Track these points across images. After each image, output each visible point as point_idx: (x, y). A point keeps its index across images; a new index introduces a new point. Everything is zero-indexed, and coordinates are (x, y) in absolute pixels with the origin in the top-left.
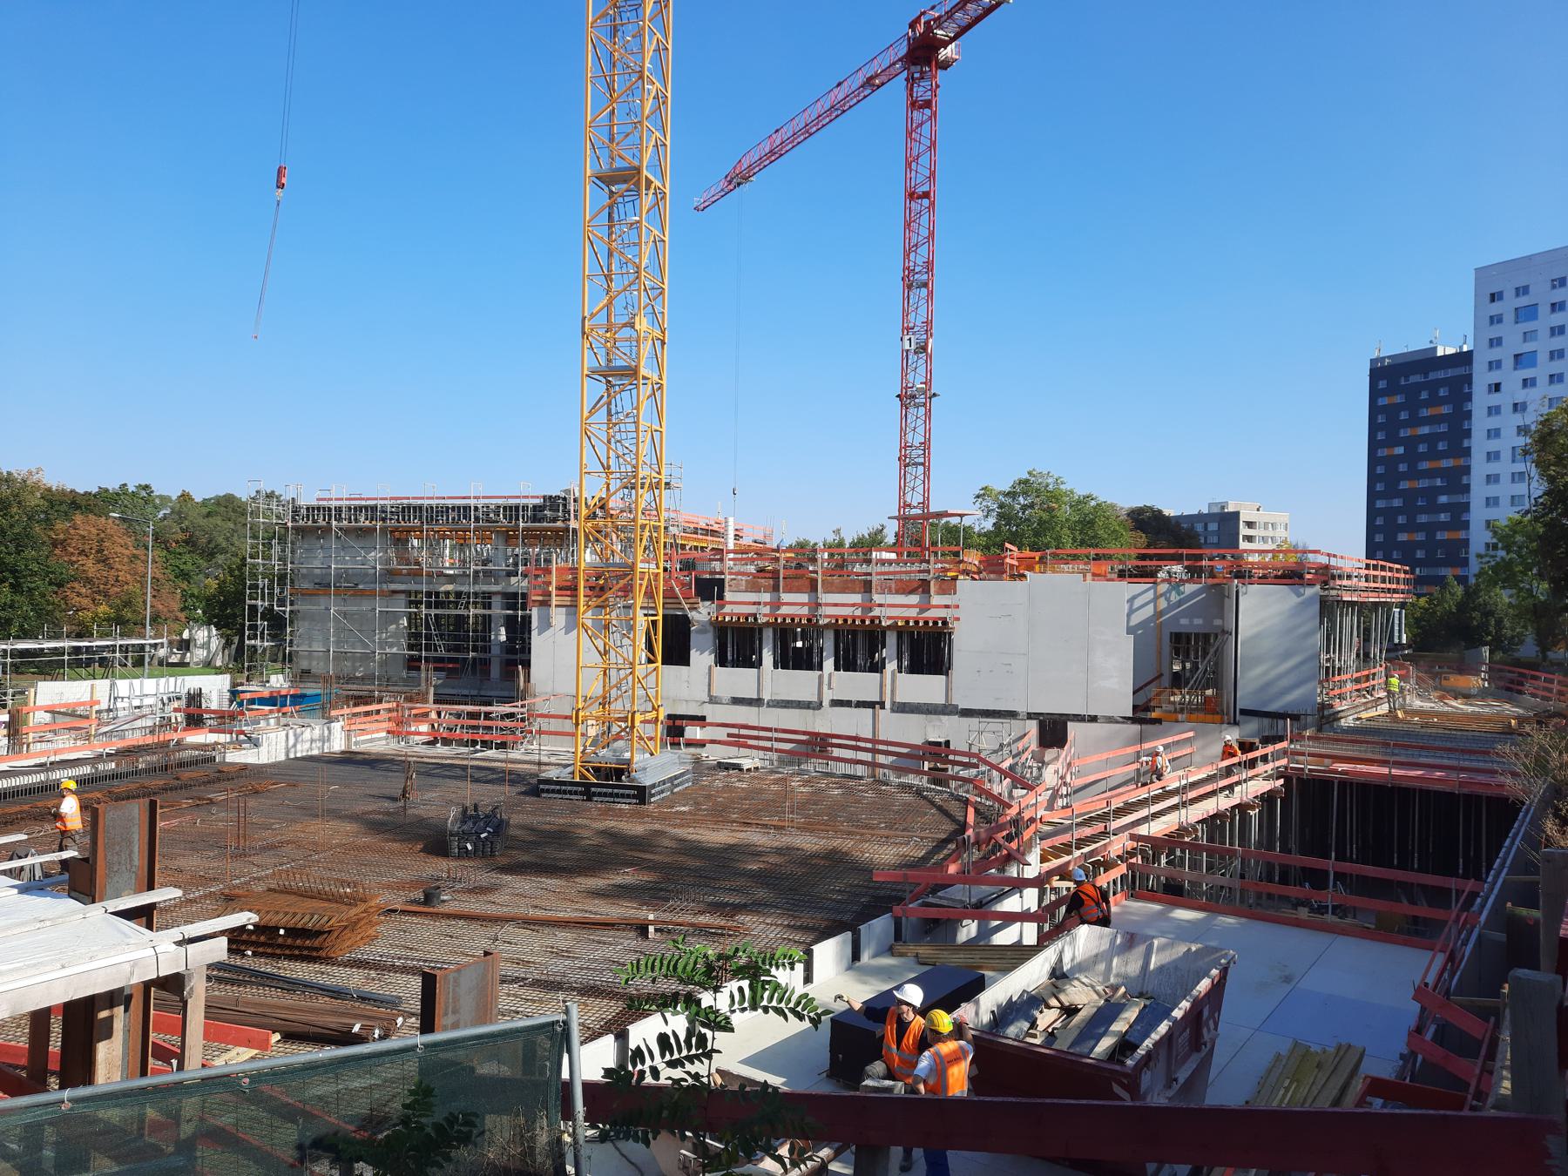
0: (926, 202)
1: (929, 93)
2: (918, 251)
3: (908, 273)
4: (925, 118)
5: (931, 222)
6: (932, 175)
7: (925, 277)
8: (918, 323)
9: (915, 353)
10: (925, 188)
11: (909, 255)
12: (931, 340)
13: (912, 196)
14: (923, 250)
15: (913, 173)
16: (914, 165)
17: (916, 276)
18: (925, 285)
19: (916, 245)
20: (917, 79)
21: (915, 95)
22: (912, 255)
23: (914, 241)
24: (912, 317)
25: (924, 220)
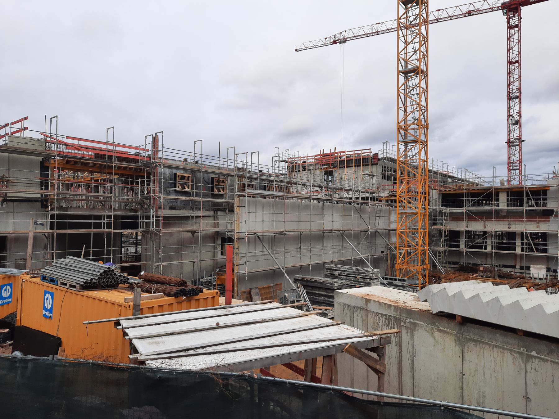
0: (517, 65)
2: (514, 84)
7: (518, 94)
10: (517, 59)
11: (509, 87)
13: (510, 63)
14: (517, 84)
15: (511, 54)
16: (511, 51)
18: (517, 97)
19: (513, 82)
22: (511, 87)
23: (512, 80)
25: (517, 72)
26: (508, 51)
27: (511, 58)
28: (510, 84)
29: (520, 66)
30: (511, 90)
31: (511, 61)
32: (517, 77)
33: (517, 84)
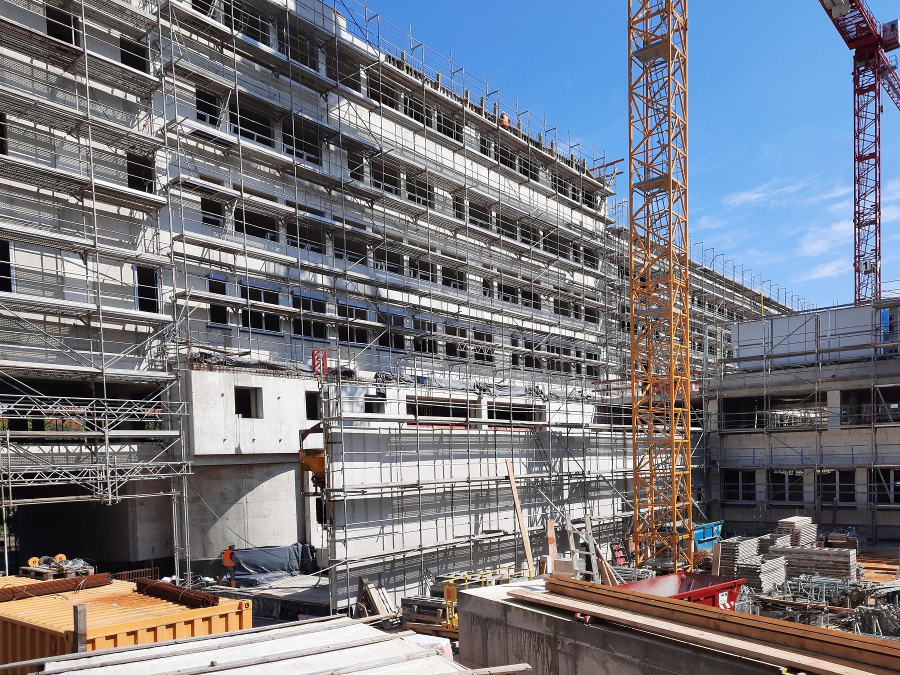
0: (872, 161)
1: (874, 79)
2: (866, 198)
3: (858, 215)
4: (870, 98)
5: (878, 175)
6: (878, 139)
8: (869, 251)
9: (866, 273)
10: (873, 151)
11: (858, 203)
12: (879, 263)
13: (859, 158)
14: (871, 198)
16: (861, 136)
17: (865, 217)
18: (873, 222)
19: (865, 194)
20: (862, 71)
21: (861, 83)
22: (862, 203)
23: (863, 190)
24: (863, 248)
25: (872, 175)
26: (856, 137)
27: (861, 150)
28: (859, 198)
29: (878, 162)
30: (861, 209)
31: (862, 155)
32: (873, 184)
33: (871, 198)
